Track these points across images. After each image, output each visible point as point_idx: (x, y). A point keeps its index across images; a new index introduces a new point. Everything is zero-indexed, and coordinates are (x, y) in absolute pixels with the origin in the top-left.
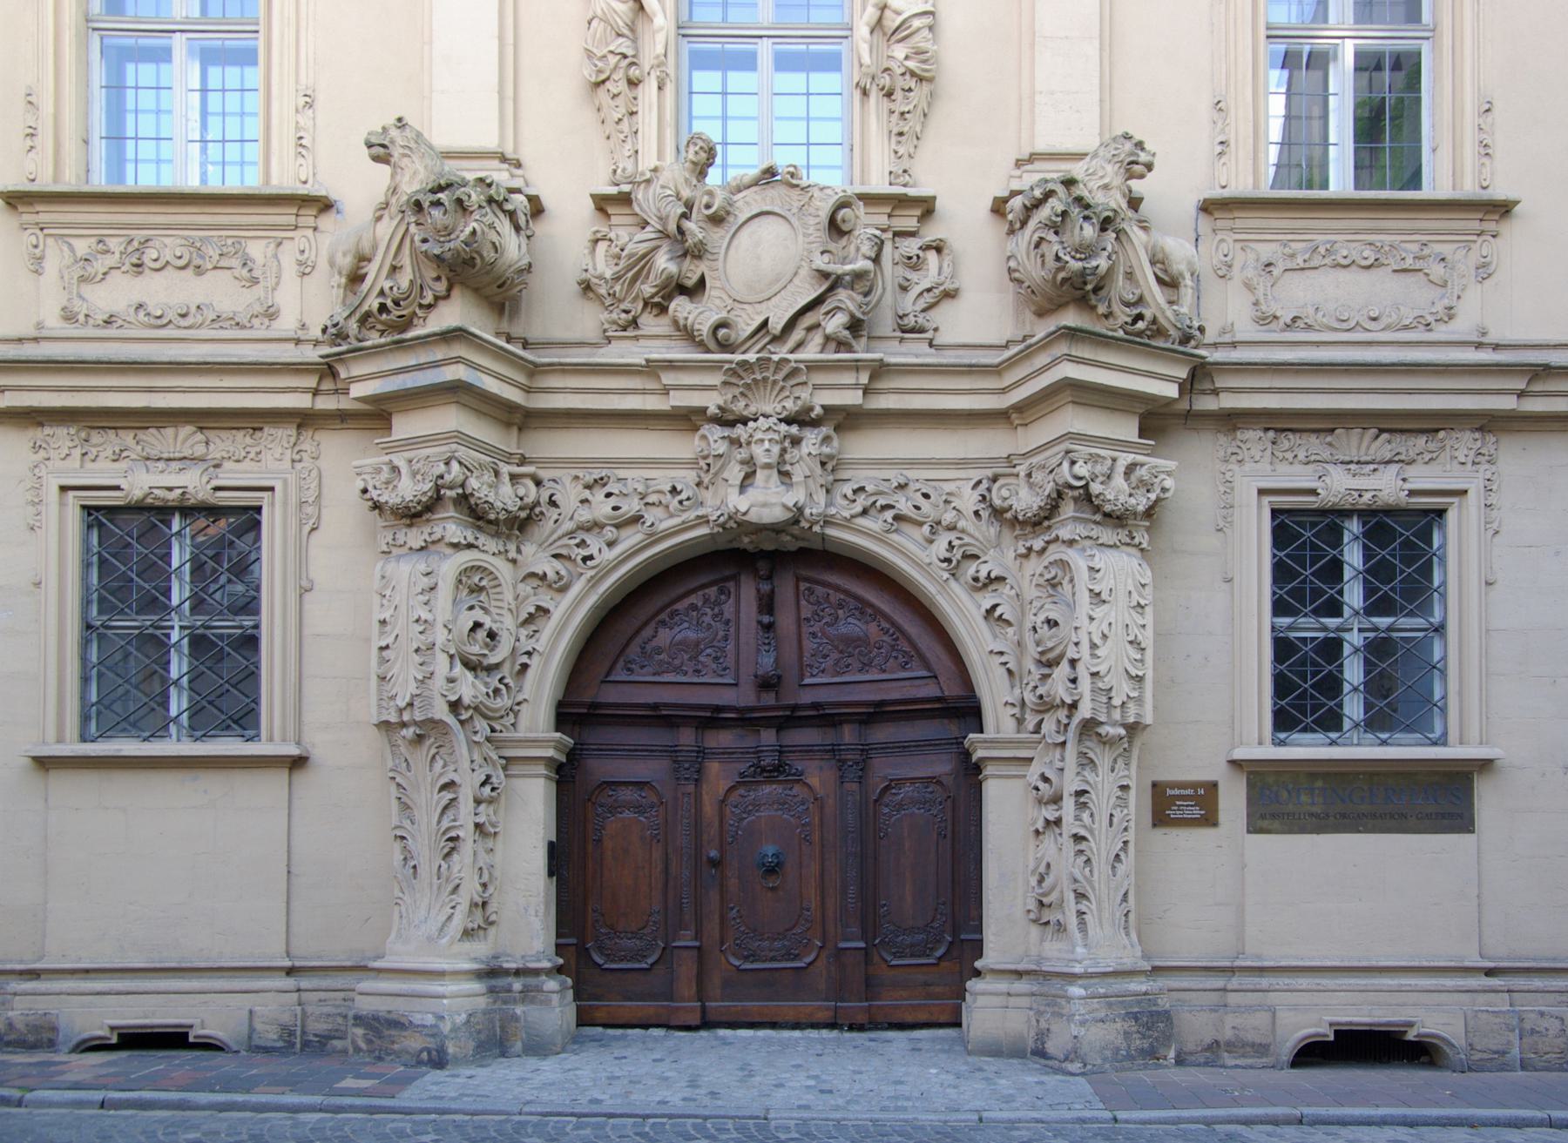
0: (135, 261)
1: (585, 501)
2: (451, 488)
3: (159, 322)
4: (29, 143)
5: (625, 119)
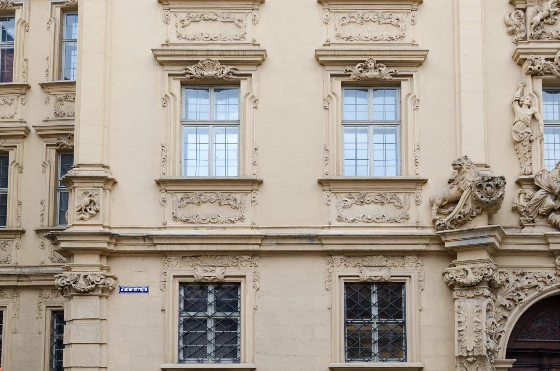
0: (362, 201)
1: (517, 280)
2: (488, 278)
3: (370, 221)
4: (326, 162)
5: (528, 153)
